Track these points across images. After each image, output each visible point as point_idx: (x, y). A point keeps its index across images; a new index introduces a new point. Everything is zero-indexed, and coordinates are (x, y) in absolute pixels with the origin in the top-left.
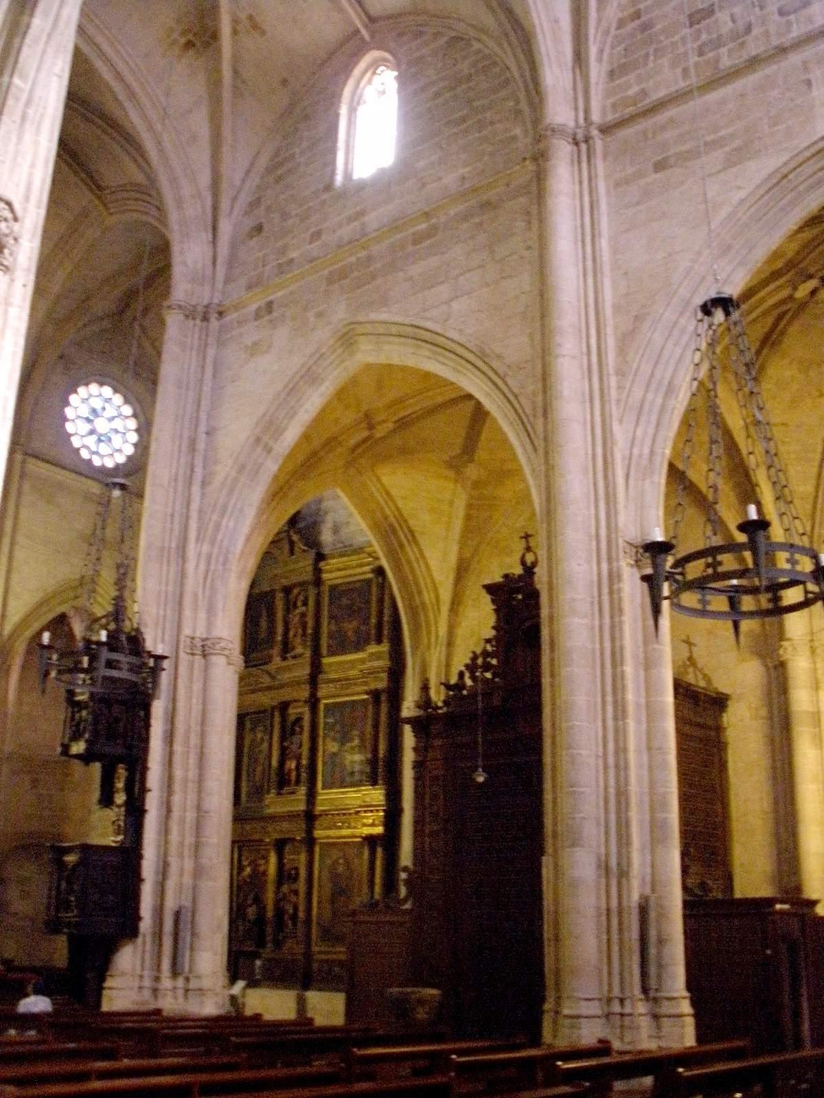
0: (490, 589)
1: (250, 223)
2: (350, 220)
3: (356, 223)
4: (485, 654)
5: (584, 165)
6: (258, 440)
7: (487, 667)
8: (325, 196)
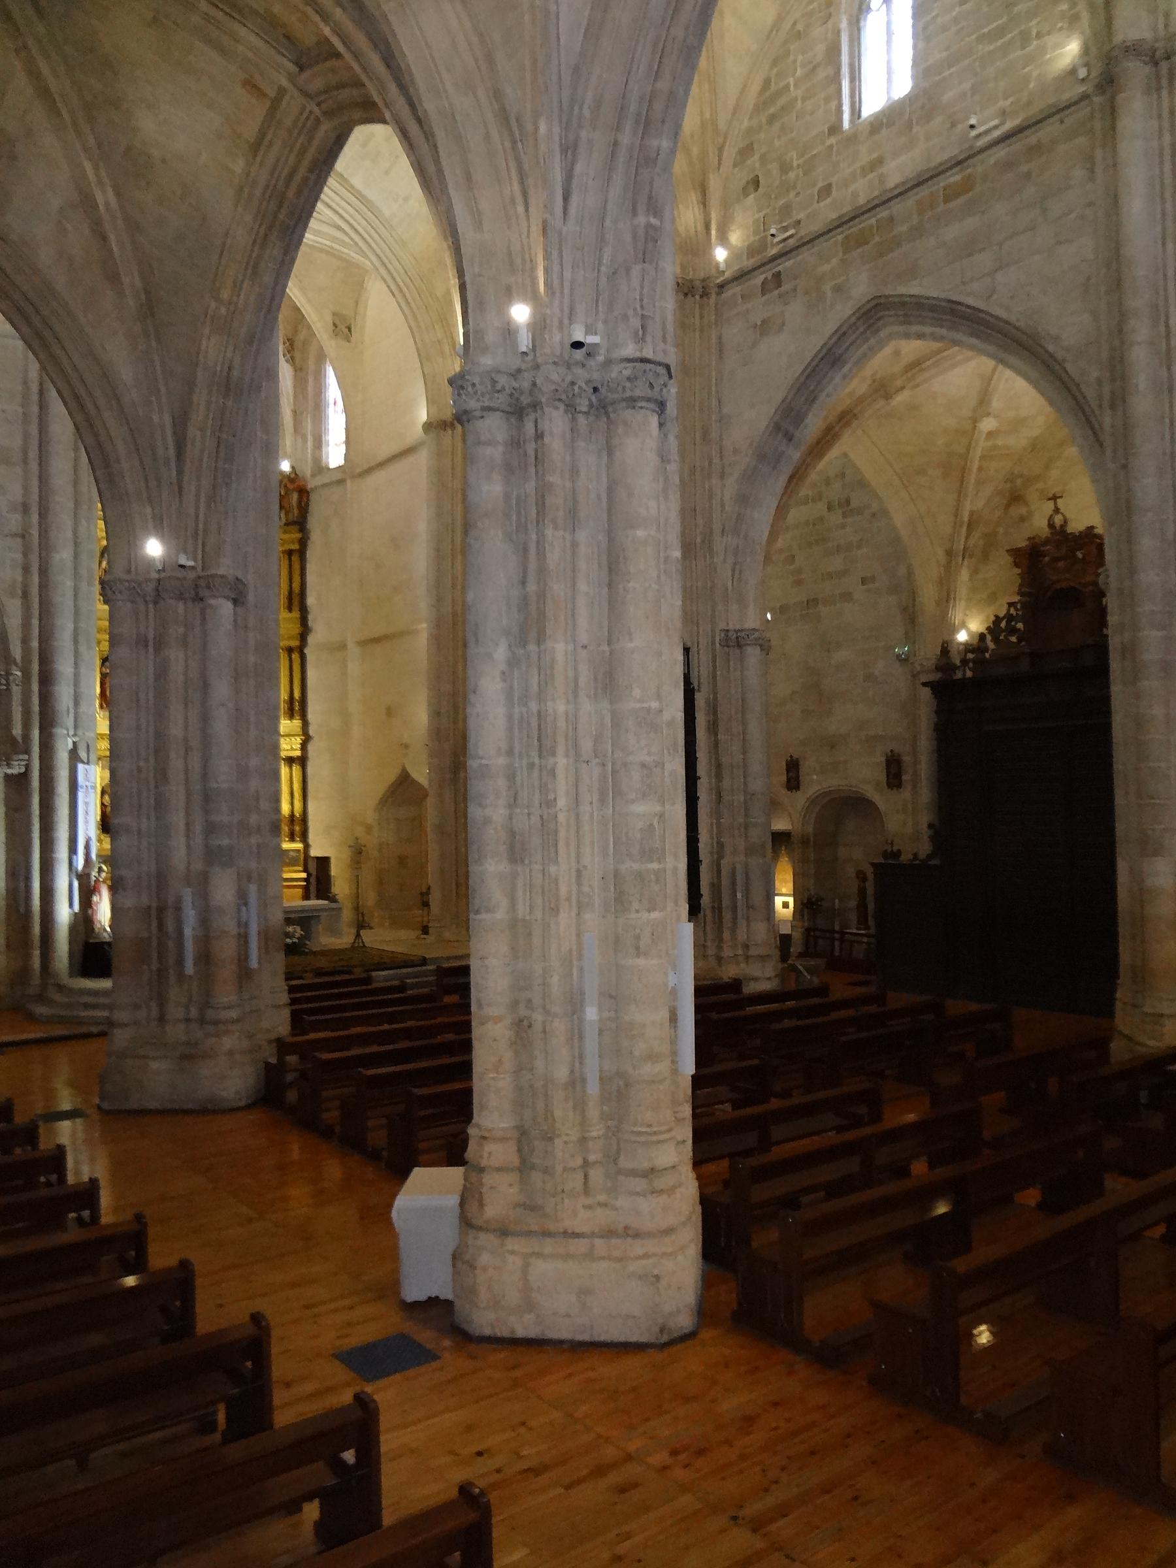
0: (1015, 553)
1: (741, 177)
2: (864, 171)
3: (871, 176)
4: (1009, 618)
5: (1165, 93)
6: (777, 427)
7: (1012, 631)
8: (832, 140)
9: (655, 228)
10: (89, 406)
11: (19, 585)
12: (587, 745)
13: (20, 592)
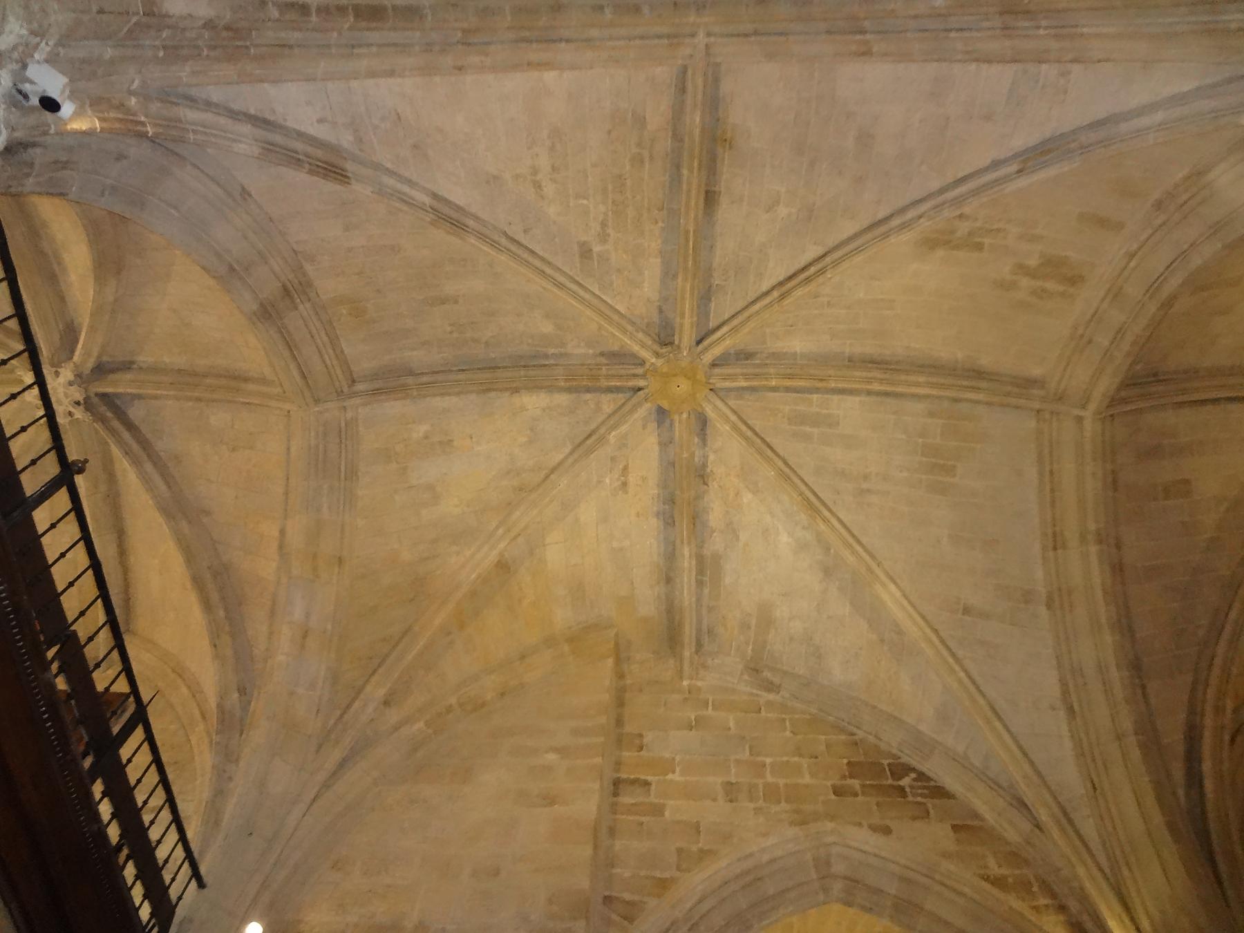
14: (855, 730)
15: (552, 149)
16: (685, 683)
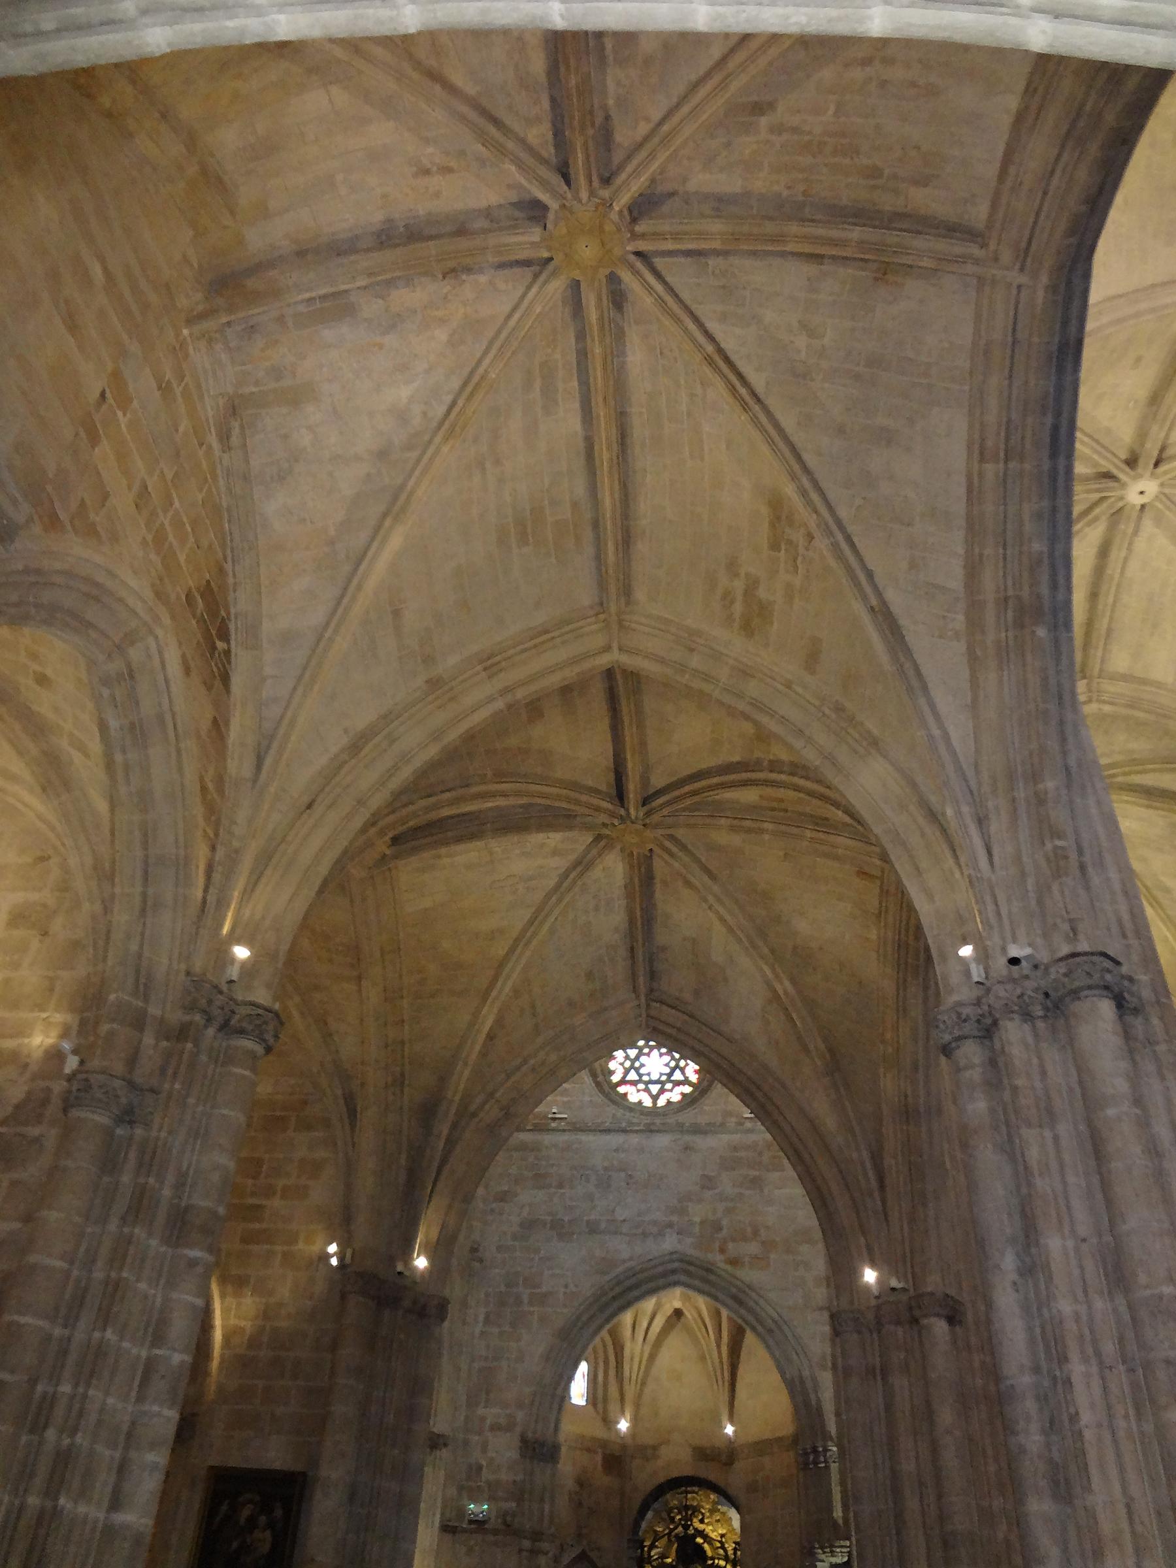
9: (1062, 848)
10: (806, 1156)
11: (829, 1358)
12: (1109, 1348)
13: (830, 1364)
14: (229, 559)
15: (913, 84)
16: (185, 332)
